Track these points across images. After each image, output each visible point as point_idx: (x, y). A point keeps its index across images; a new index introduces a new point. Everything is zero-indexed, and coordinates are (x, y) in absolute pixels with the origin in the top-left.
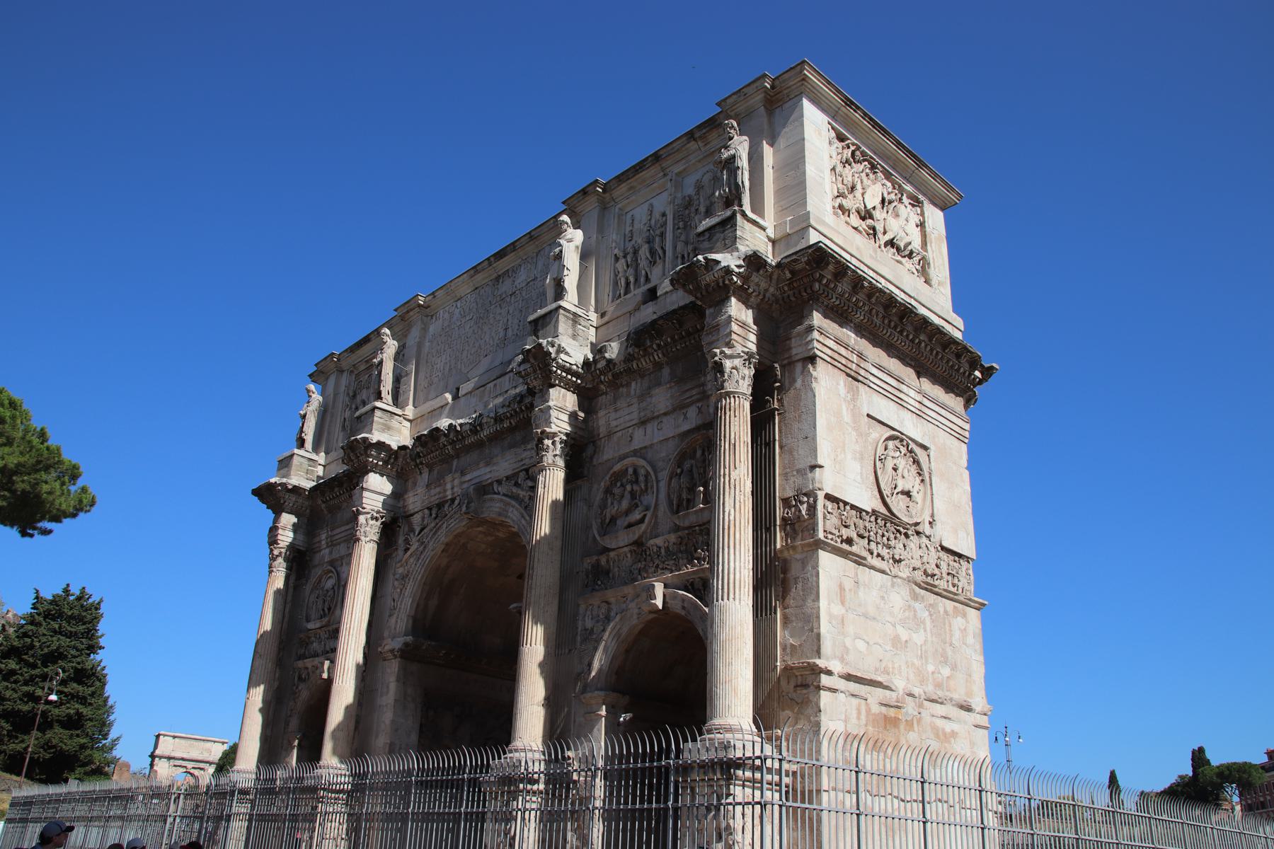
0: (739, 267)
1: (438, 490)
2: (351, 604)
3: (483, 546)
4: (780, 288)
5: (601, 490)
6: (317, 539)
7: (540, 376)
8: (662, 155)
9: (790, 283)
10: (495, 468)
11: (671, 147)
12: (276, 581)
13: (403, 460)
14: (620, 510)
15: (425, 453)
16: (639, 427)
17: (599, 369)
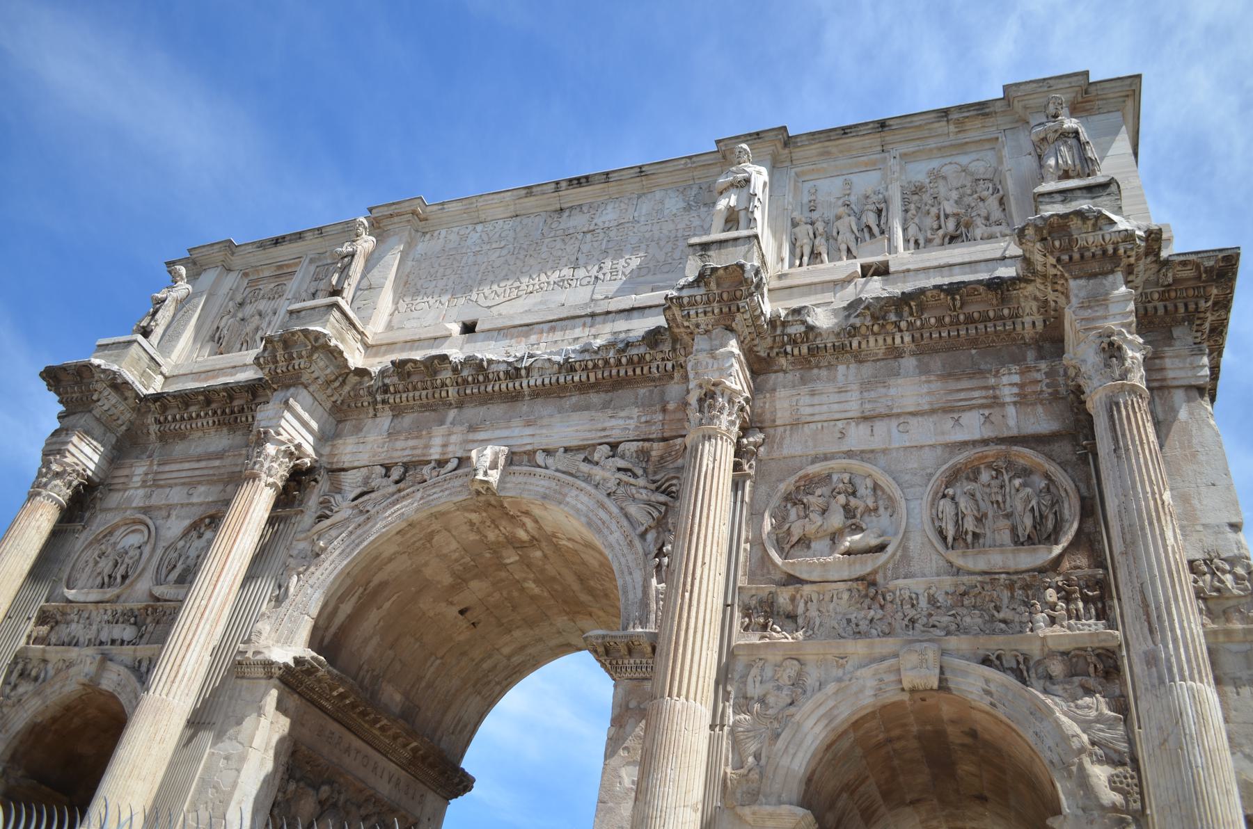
0: (1140, 238)
1: (411, 443)
2: (216, 574)
3: (454, 545)
4: (1146, 294)
5: (779, 494)
6: (126, 472)
7: (716, 311)
8: (890, 126)
9: (1163, 292)
10: (544, 431)
11: (908, 120)
12: (40, 512)
13: (353, 389)
14: (825, 527)
15: (401, 387)
16: (857, 424)
17: (789, 335)
